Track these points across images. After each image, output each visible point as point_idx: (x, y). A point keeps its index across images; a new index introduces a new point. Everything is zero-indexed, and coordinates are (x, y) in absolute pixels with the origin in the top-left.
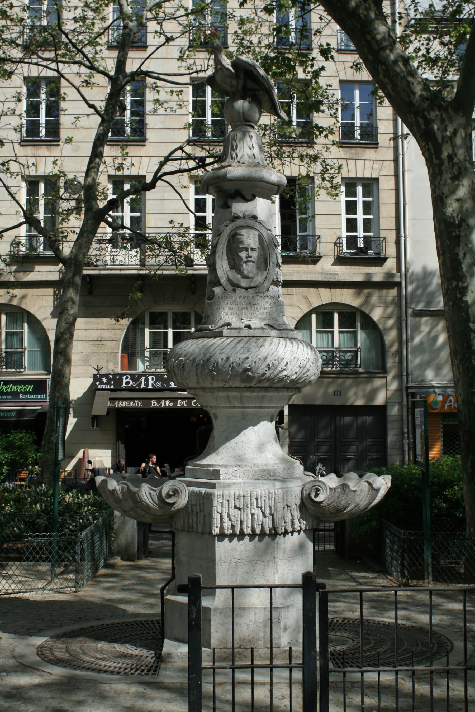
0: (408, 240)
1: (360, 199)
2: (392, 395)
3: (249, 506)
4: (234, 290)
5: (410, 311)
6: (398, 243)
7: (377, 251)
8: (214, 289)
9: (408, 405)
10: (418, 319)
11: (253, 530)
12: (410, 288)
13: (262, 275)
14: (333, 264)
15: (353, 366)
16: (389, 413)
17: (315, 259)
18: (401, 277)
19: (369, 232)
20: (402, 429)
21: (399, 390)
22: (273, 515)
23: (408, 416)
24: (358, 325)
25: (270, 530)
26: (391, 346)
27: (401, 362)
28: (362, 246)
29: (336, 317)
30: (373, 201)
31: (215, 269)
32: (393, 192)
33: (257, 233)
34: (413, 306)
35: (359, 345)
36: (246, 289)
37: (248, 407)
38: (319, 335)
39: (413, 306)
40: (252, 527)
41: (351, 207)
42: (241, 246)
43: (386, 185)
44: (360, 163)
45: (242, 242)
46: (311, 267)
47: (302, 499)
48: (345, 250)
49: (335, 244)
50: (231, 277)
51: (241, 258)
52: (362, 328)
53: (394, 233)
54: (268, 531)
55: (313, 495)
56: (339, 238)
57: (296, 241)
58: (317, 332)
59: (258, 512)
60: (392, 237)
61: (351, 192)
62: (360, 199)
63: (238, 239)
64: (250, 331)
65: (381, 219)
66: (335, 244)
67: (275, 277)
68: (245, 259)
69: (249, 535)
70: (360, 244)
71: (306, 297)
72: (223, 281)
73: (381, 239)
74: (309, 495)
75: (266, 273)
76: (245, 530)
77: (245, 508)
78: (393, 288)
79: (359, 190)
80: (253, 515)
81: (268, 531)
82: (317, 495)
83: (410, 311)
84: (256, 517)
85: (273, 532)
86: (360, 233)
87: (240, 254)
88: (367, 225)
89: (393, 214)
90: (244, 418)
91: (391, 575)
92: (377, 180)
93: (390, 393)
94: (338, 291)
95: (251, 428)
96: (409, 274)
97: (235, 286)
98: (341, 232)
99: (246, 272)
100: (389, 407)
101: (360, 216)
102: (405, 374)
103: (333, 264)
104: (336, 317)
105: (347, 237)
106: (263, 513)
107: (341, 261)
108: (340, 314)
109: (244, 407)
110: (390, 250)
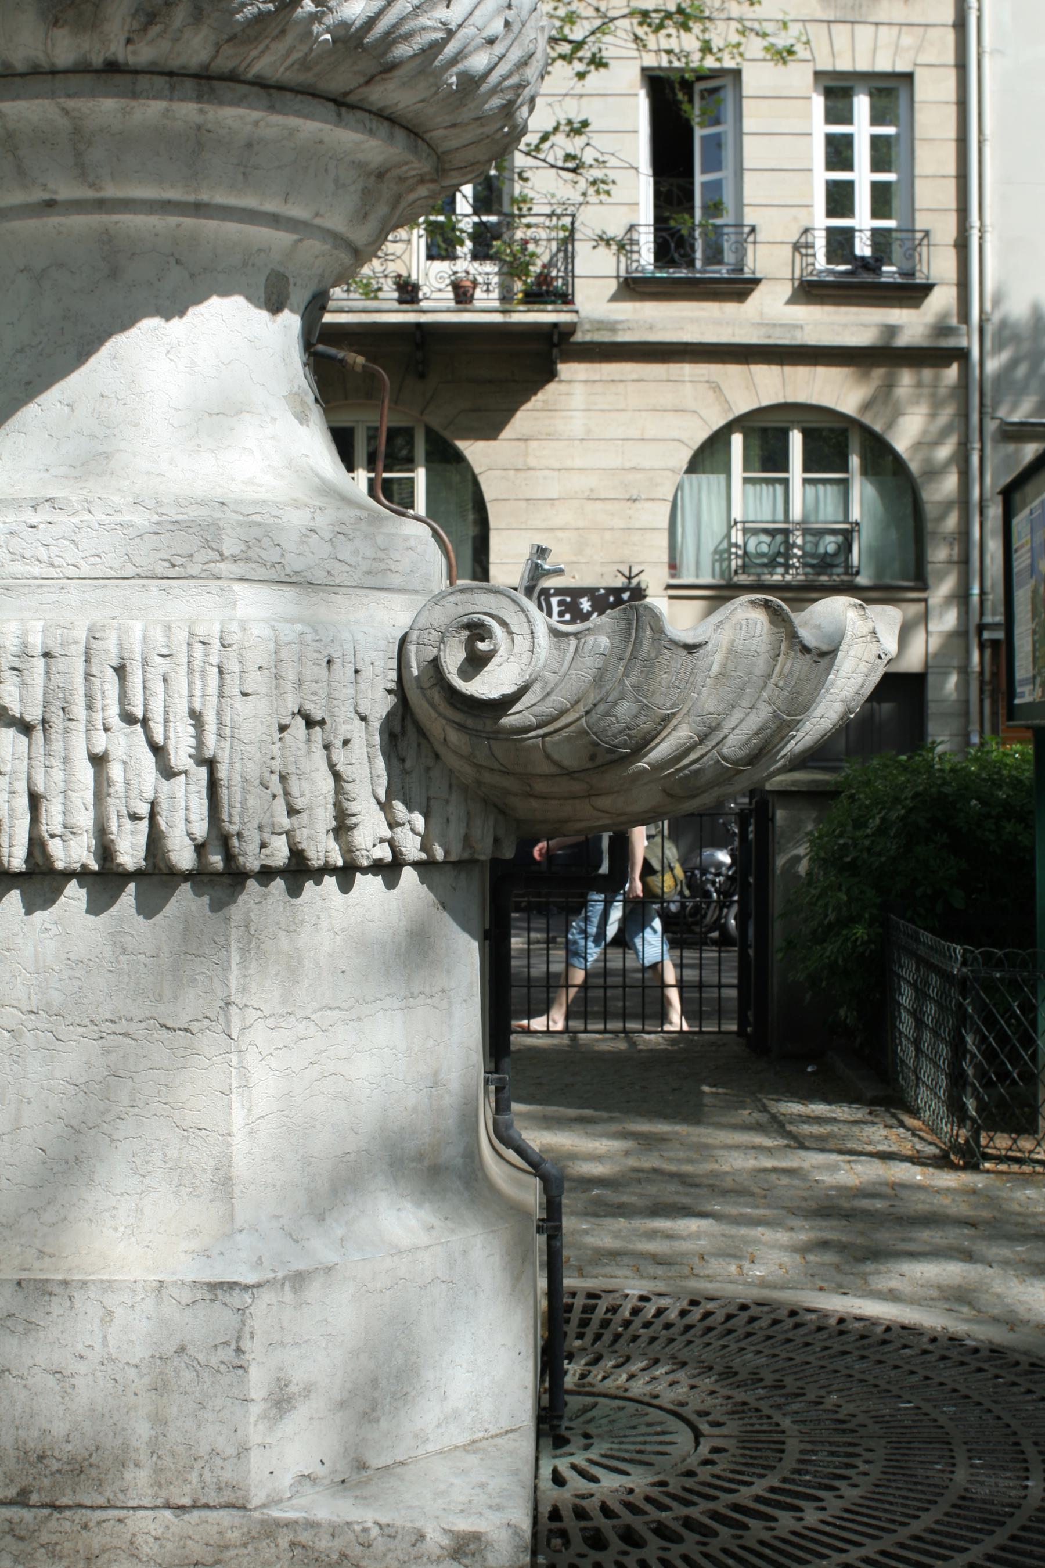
0: (988, 237)
1: (862, 129)
2: (944, 646)
3: (79, 710)
5: (991, 426)
6: (962, 245)
7: (907, 267)
9: (982, 673)
10: (1011, 447)
11: (105, 851)
12: (992, 365)
14: (792, 301)
15: (840, 570)
16: (931, 694)
17: (739, 288)
18: (969, 335)
19: (887, 216)
20: (967, 736)
21: (961, 634)
22: (211, 764)
23: (981, 701)
24: (855, 461)
25: (200, 849)
26: (942, 517)
27: (964, 561)
28: (867, 252)
29: (796, 440)
30: (898, 135)
32: (952, 111)
34: (1002, 413)
35: (855, 514)
37: (127, 205)
38: (750, 488)
39: (1002, 413)
40: (101, 831)
41: (839, 152)
43: (934, 91)
44: (864, 33)
46: (730, 309)
47: (400, 690)
48: (821, 262)
49: (796, 247)
52: (865, 472)
53: (952, 219)
54: (183, 857)
55: (453, 659)
56: (806, 231)
57: (689, 240)
58: (746, 481)
59: (128, 748)
60: (945, 230)
61: (838, 109)
62: (862, 129)
65: (918, 183)
66: (796, 247)
69: (82, 875)
70: (863, 248)
71: (716, 388)
73: (919, 235)
74: (435, 663)
76: (55, 847)
77: (57, 720)
78: (948, 365)
79: (862, 104)
80: (99, 761)
81: (183, 857)
82: (475, 663)
83: (991, 426)
84: (115, 771)
85: (216, 860)
86: (862, 219)
88: (882, 199)
89: (951, 169)
90: (114, 273)
91: (915, 1113)
92: (908, 77)
93: (934, 643)
94: (801, 372)
95: (150, 324)
96: (989, 329)
98: (811, 215)
100: (931, 680)
101: (862, 176)
102: (976, 590)
103: (792, 301)
104: (796, 440)
105: (830, 231)
106: (158, 750)
107: (810, 291)
108: (807, 434)
109: (101, 205)
110: (939, 265)
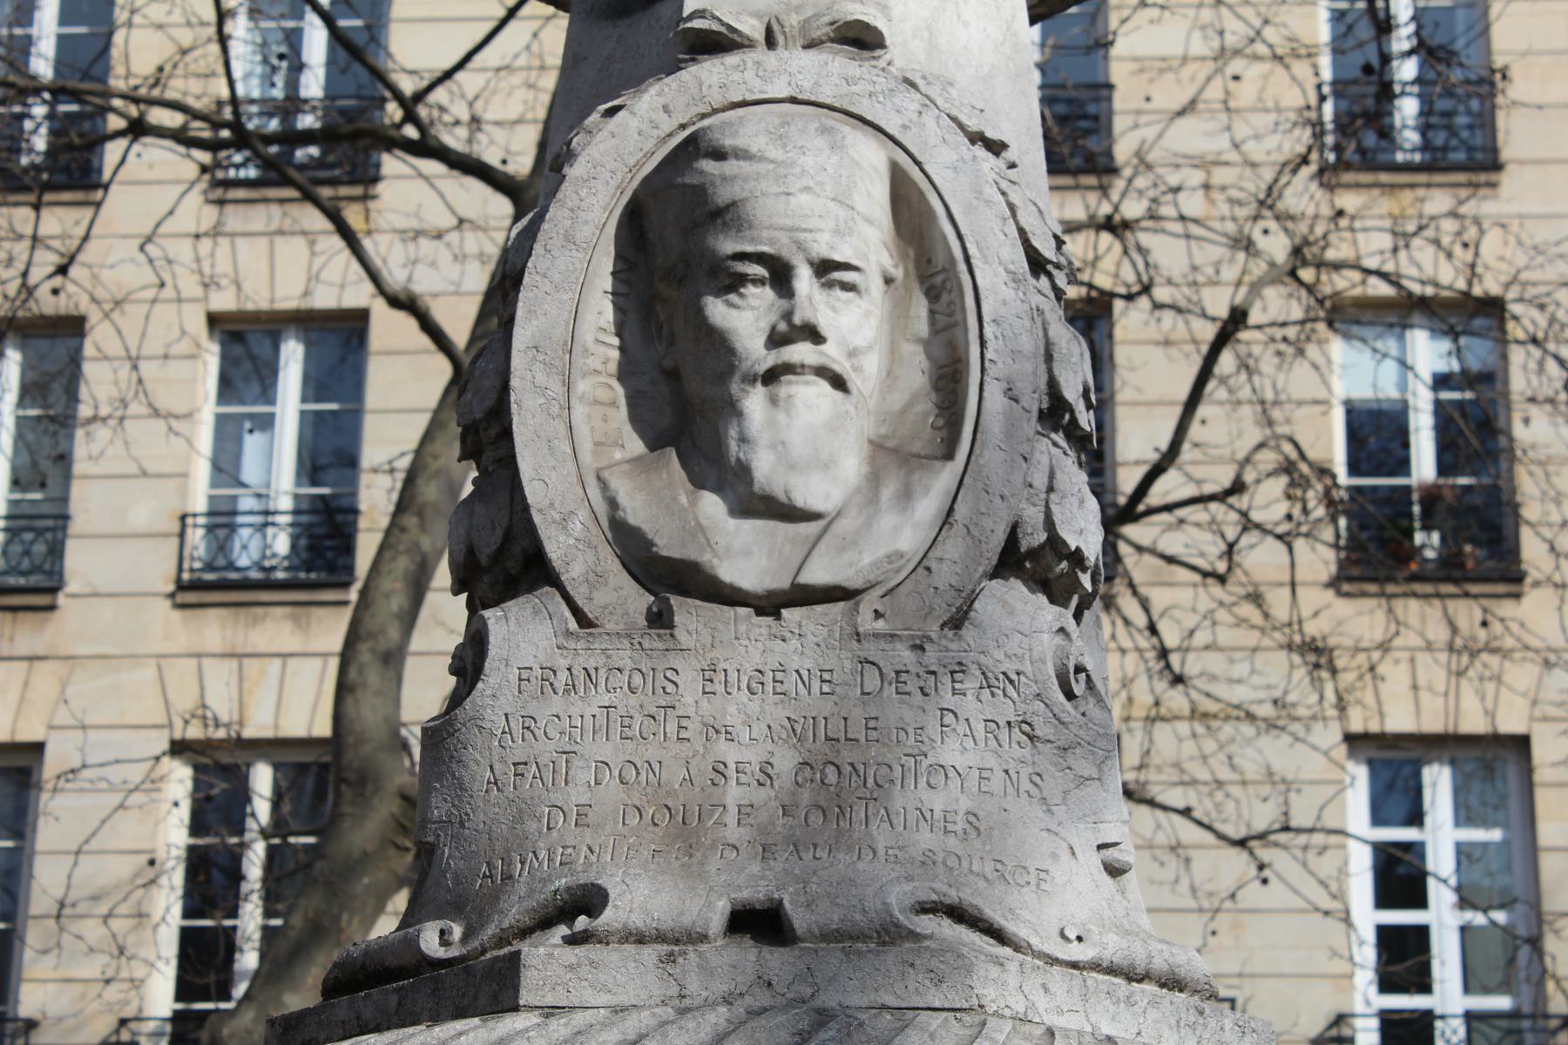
4: (660, 619)
8: (487, 613)
13: (906, 496)
31: (509, 461)
33: (872, 156)
36: (769, 605)
42: (727, 245)
45: (725, 215)
50: (636, 511)
51: (719, 345)
63: (700, 193)
64: (776, 959)
67: (1033, 515)
68: (768, 360)
72: (570, 538)
75: (947, 475)
87: (717, 310)
97: (671, 580)
99: (765, 468)
